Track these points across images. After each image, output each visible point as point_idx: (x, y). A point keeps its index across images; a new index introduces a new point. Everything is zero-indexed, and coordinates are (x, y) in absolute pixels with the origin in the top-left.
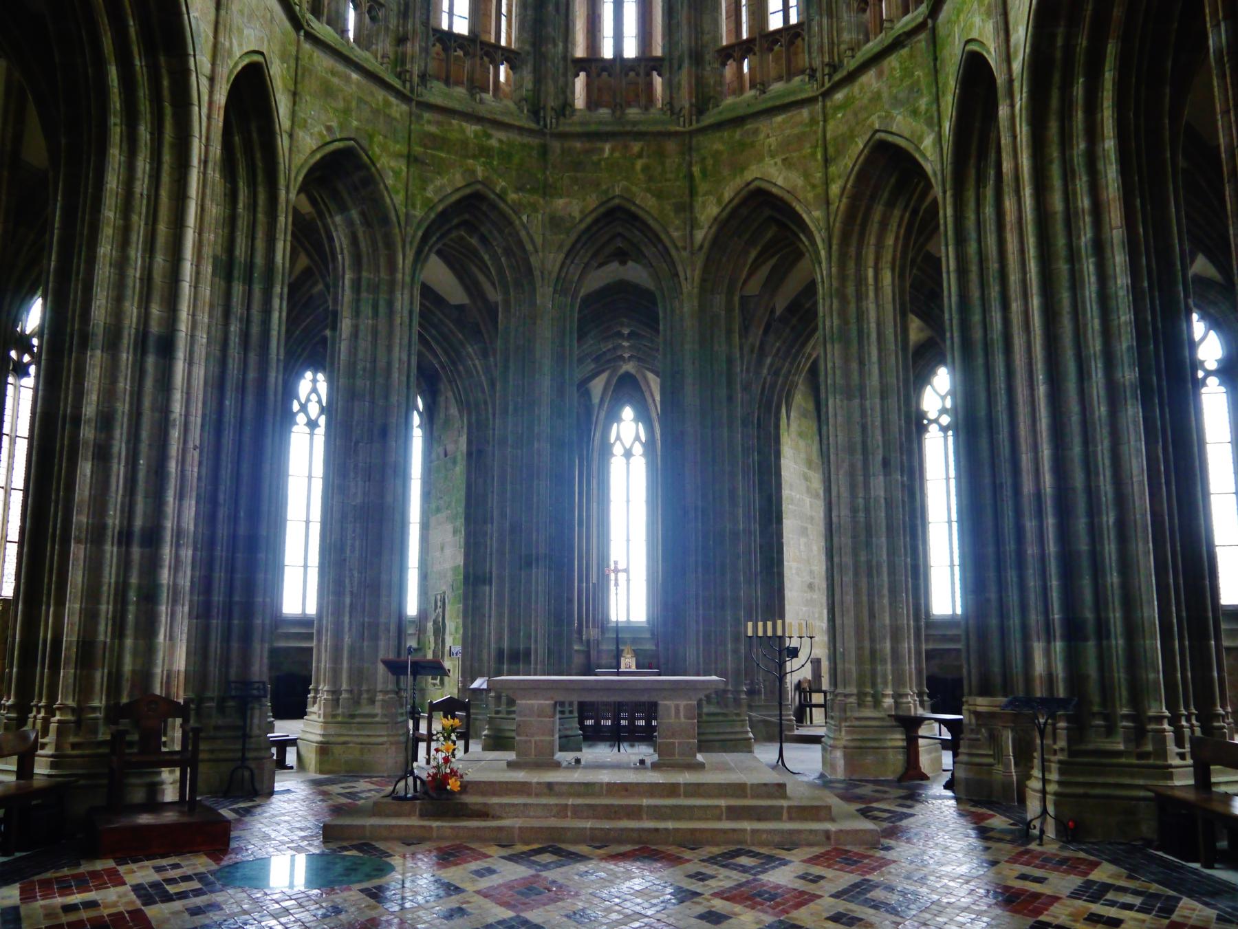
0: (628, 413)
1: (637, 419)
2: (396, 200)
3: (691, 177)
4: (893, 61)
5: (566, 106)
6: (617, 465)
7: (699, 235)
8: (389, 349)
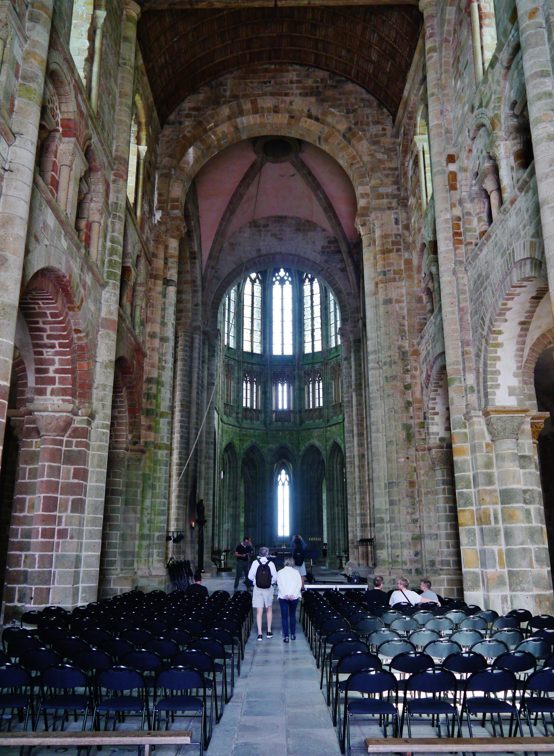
0: (283, 472)
2: (238, 450)
4: (338, 426)
5: (271, 422)
7: (301, 453)
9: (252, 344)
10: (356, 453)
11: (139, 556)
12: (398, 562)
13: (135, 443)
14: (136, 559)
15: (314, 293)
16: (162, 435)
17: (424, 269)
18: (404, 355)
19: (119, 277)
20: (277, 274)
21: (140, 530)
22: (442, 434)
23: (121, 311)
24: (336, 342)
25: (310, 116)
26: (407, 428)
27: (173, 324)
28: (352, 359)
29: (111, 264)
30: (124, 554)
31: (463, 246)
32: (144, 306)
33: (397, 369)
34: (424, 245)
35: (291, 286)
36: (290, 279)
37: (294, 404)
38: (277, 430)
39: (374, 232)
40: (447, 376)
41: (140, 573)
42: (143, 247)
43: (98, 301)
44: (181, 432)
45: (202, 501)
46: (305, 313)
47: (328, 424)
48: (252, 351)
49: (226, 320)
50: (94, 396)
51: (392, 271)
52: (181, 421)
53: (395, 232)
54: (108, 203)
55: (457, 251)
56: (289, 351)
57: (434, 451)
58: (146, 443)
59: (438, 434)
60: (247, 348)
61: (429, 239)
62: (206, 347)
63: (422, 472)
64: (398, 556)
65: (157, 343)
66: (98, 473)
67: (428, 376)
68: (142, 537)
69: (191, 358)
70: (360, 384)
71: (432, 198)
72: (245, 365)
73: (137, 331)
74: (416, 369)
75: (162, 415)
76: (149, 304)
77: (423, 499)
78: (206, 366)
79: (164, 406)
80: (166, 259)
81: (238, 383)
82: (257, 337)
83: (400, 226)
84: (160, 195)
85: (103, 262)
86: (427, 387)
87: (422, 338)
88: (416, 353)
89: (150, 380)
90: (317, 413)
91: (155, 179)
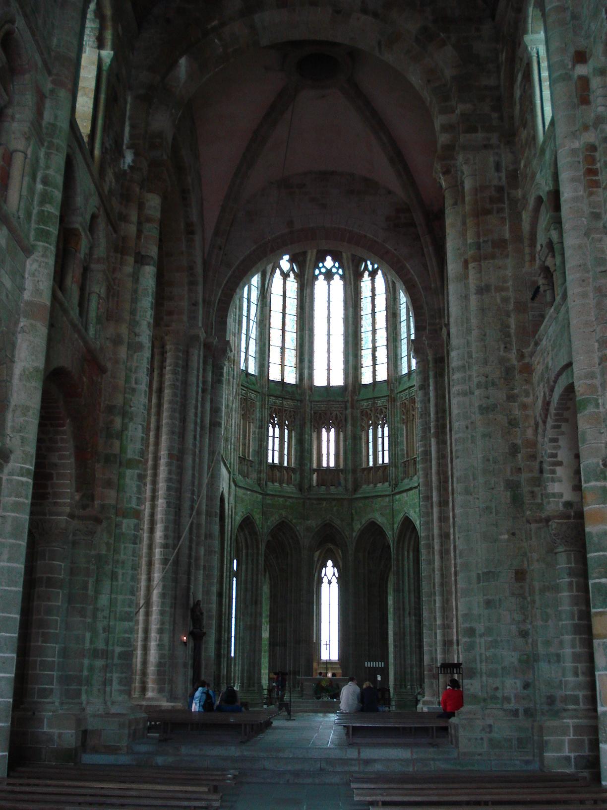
0: (330, 563)
1: (334, 567)
3: (352, 514)
4: (411, 492)
5: (311, 486)
6: (325, 587)
7: (354, 534)
8: (257, 575)
9: (283, 369)
10: (436, 531)
11: (89, 683)
12: (496, 698)
13: (84, 507)
14: (84, 688)
15: (377, 292)
16: (128, 495)
17: (541, 239)
18: (508, 372)
19: (54, 239)
20: (321, 265)
21: (91, 642)
22: (568, 496)
23: (60, 294)
24: (409, 366)
25: (364, 11)
26: (513, 486)
27: (149, 323)
28: (431, 388)
29: (43, 218)
30: (65, 680)
31: (600, 190)
32: (103, 294)
33: (499, 395)
34: (539, 200)
35: (342, 282)
36: (340, 272)
37: (345, 459)
38: (319, 499)
39: (462, 183)
40: (575, 396)
41: (90, 710)
42: (102, 201)
43: (18, 275)
44: (168, 497)
45: (197, 604)
46: (363, 323)
47: (397, 491)
48: (283, 379)
49: (244, 331)
50: (9, 424)
51: (490, 243)
52: (169, 480)
53: (495, 182)
54: (40, 125)
55: (592, 198)
56: (338, 380)
57: (553, 524)
58: (103, 507)
59: (561, 495)
60: (274, 375)
61: (547, 189)
62: (209, 368)
63: (535, 556)
64: (497, 689)
65: (123, 352)
66: (12, 546)
67: (547, 404)
68: (96, 654)
69: (185, 383)
70: (444, 426)
71: (552, 123)
72: (272, 399)
73: (92, 331)
74: (527, 395)
75: (130, 464)
76: (112, 292)
77: (537, 598)
78: (209, 397)
79: (132, 450)
80: (140, 223)
81: (261, 427)
82: (291, 358)
83: (503, 175)
84: (133, 127)
85: (29, 215)
86: (545, 422)
87: (537, 344)
88: (528, 369)
89: (111, 409)
90: (380, 473)
91: (126, 103)
